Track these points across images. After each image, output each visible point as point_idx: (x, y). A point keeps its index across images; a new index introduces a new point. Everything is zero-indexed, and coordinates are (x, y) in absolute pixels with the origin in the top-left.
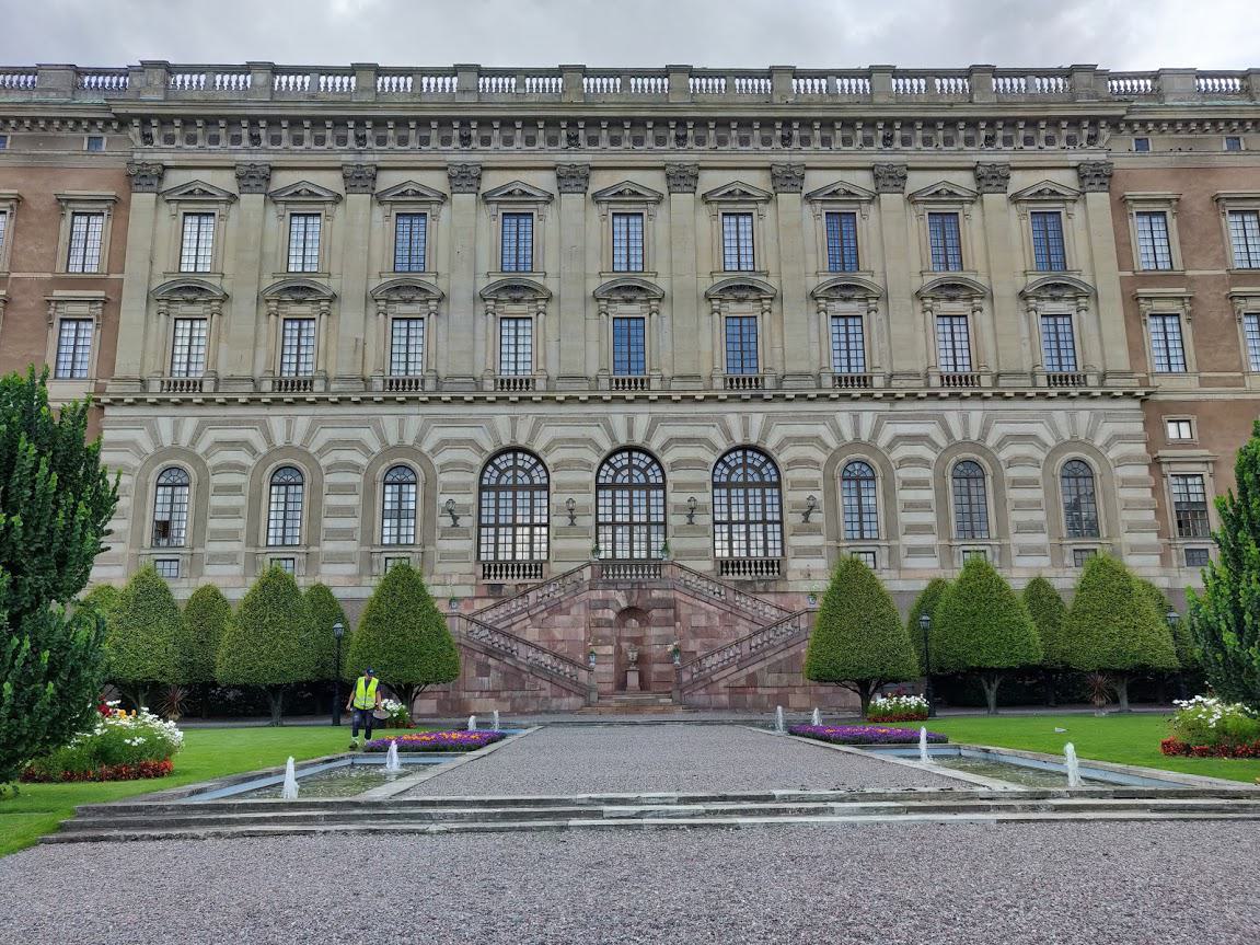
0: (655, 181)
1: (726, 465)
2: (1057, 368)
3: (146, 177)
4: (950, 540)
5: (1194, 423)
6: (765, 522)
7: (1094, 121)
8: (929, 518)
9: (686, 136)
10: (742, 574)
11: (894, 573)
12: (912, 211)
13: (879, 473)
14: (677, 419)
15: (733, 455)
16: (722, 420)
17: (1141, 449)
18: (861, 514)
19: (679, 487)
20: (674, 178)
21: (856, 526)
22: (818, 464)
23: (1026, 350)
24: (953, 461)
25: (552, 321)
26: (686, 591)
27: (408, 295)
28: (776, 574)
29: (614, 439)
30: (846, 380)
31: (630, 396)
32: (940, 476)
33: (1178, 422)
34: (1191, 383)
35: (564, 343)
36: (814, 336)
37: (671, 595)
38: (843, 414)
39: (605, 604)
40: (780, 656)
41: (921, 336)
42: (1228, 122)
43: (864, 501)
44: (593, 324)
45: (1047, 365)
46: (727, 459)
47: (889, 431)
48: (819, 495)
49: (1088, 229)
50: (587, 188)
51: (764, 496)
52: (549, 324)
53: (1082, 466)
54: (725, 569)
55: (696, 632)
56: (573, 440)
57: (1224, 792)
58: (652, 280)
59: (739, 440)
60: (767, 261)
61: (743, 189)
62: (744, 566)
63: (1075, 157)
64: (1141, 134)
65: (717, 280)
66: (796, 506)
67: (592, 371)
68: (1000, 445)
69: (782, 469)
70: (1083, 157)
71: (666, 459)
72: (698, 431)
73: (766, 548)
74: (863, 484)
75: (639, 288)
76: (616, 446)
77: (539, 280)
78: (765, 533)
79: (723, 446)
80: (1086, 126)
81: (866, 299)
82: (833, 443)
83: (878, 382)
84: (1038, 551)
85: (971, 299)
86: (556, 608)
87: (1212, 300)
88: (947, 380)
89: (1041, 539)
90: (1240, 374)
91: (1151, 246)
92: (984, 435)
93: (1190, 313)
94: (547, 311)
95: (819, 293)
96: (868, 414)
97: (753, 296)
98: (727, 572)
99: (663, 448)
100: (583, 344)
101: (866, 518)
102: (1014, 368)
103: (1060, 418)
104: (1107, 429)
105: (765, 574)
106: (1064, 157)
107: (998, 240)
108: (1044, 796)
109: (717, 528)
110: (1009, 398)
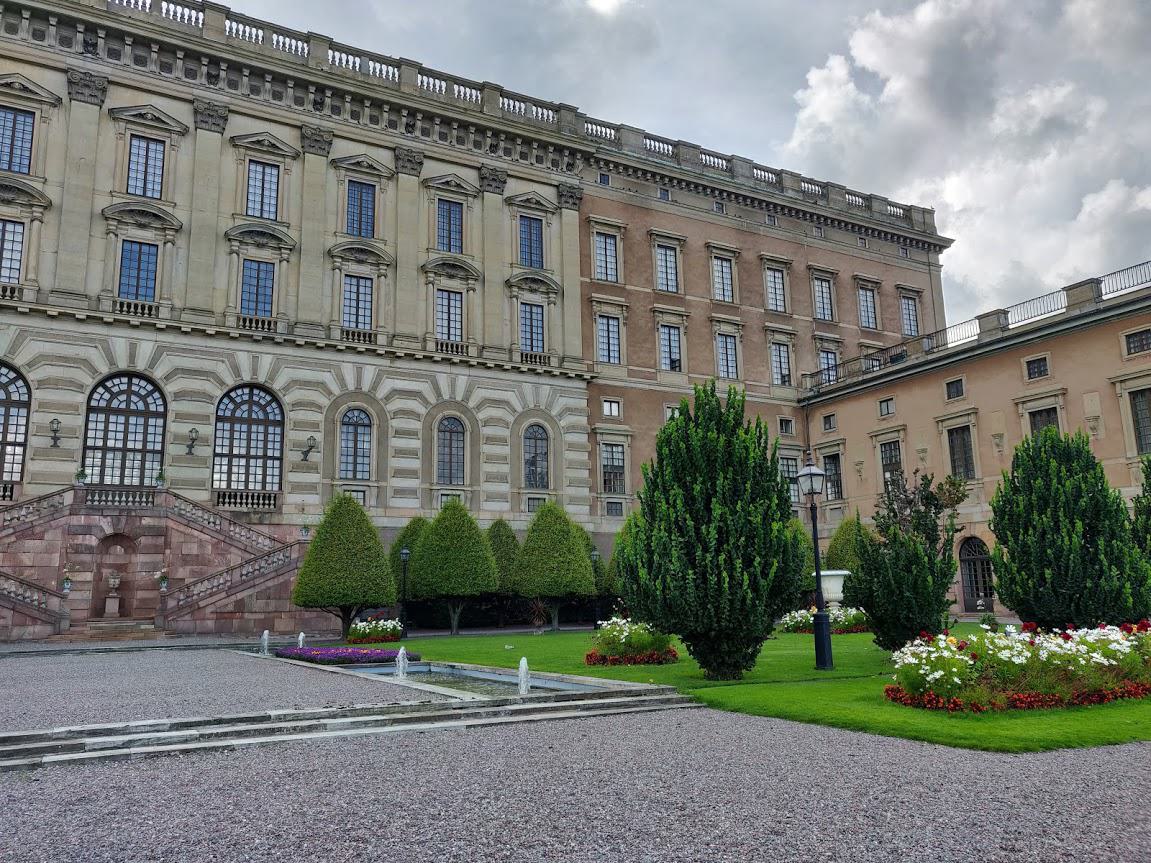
0: (182, 113)
1: (232, 400)
2: (529, 348)
4: (432, 484)
5: (621, 404)
6: (265, 457)
7: (573, 152)
8: (415, 464)
9: (219, 75)
10: (238, 505)
11: (380, 511)
12: (425, 194)
13: (375, 421)
14: (184, 350)
15: (239, 392)
16: (231, 357)
17: (583, 420)
18: (355, 455)
19: (181, 417)
20: (201, 113)
21: (350, 467)
22: (320, 407)
23: (507, 329)
24: (440, 416)
26: (180, 519)
27: (144, 220)
28: (272, 507)
29: (112, 362)
30: (353, 335)
31: (135, 321)
32: (428, 428)
33: (611, 402)
34: (622, 373)
35: (62, 256)
36: (327, 291)
37: (163, 522)
38: (348, 365)
39: (87, 530)
40: (270, 584)
41: (422, 304)
42: (663, 177)
43: (359, 445)
44: (99, 244)
45: (521, 345)
46: (233, 394)
48: (319, 437)
49: (561, 233)
50: (103, 102)
51: (266, 434)
52: (45, 233)
53: (541, 431)
54: (221, 500)
55: (186, 560)
56: (65, 359)
57: (631, 691)
58: (169, 210)
59: (247, 378)
60: (290, 213)
61: (273, 141)
62: (241, 498)
63: (557, 177)
64: (604, 171)
65: (239, 222)
66: (297, 445)
67: (94, 289)
68: (479, 407)
69: (286, 408)
70: (563, 179)
71: (170, 389)
72: (207, 365)
73: (264, 483)
74: (360, 430)
75: (155, 215)
76: (114, 370)
77: (38, 186)
78: (265, 467)
79: (231, 382)
81: (378, 265)
82: (336, 390)
83: (382, 339)
84: (502, 497)
85: (467, 279)
86: (27, 533)
87: (641, 309)
88: (441, 346)
89: (504, 488)
90: (653, 371)
91: (605, 261)
92: (467, 398)
93: (626, 319)
94: (45, 220)
95: (335, 252)
96: (370, 368)
97: (273, 243)
98: (224, 503)
99: (168, 377)
100: (85, 261)
101: (359, 460)
102: (496, 343)
103: (528, 389)
104: (562, 402)
105: (261, 506)
106: (548, 176)
108: (505, 702)
109: (217, 459)
110: (490, 368)
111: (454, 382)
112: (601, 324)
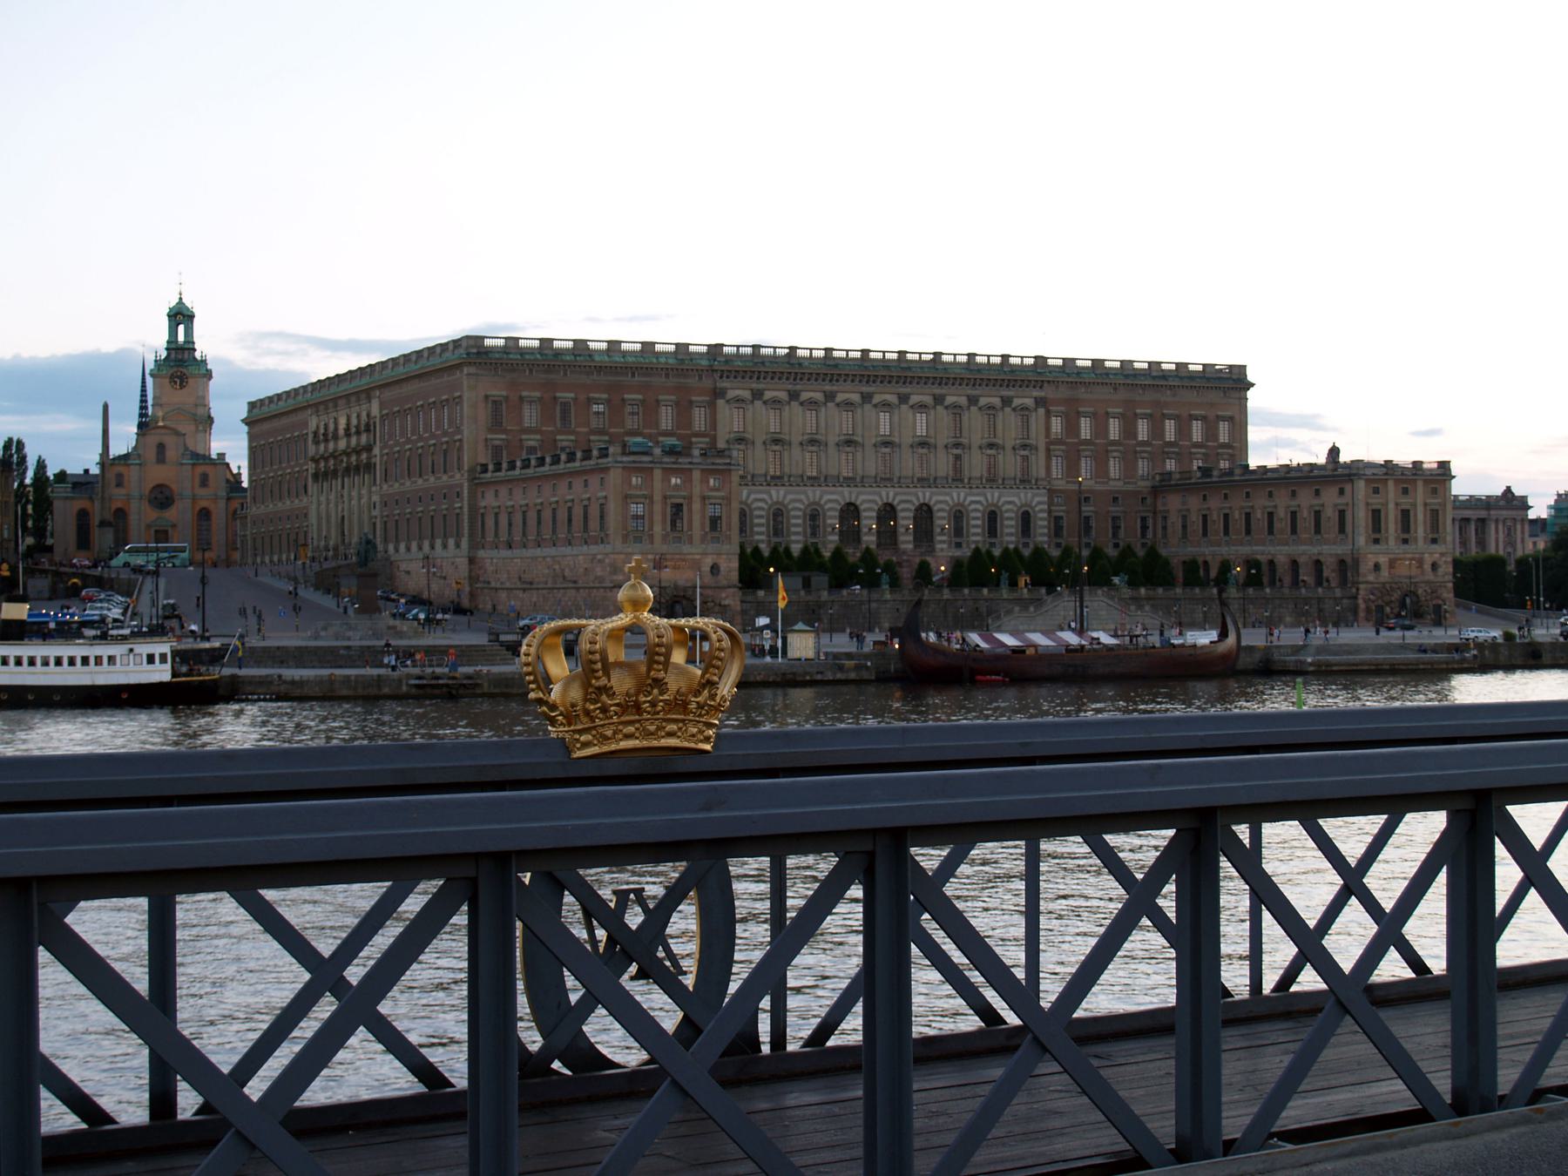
3: (718, 394)
63: (1037, 393)
104: (1037, 499)
111: (993, 495)
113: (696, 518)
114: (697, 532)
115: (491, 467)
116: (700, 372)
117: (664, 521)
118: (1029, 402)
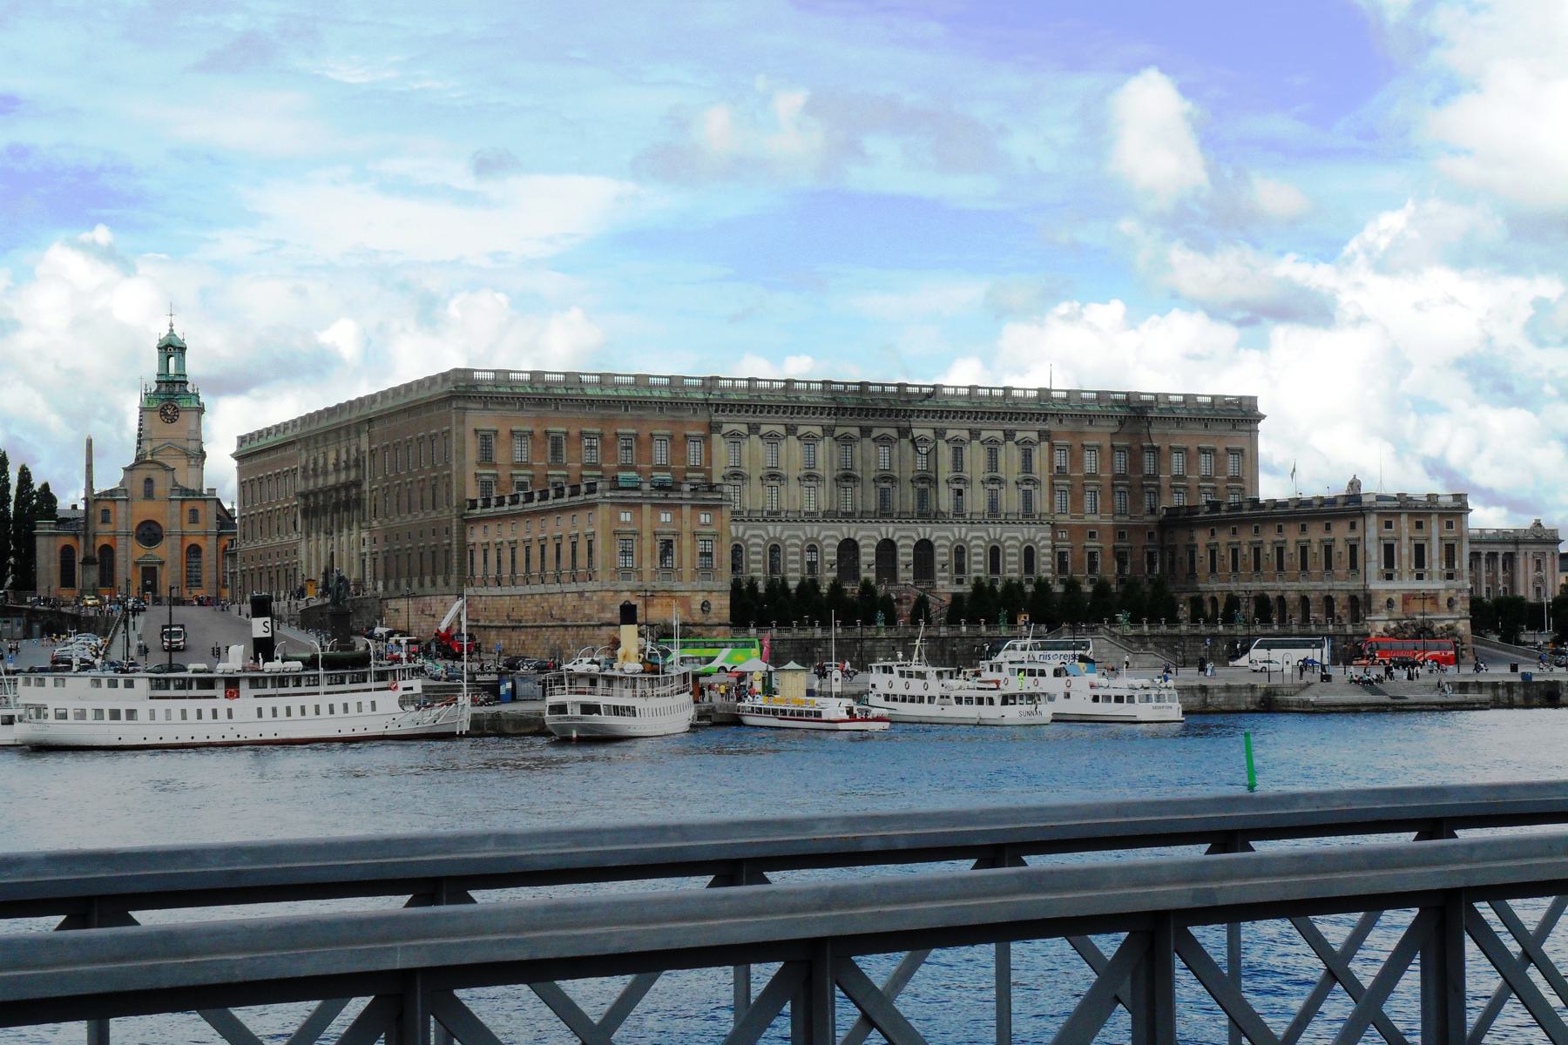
3: (713, 428)
25: (858, 489)
47: (971, 534)
49: (1040, 454)
80: (1043, 416)
91: (1060, 459)
104: (1040, 535)
107: (1010, 459)
111: (995, 531)
112: (1058, 495)
113: (686, 553)
114: (687, 570)
115: (480, 503)
116: (694, 405)
117: (653, 557)
118: (1034, 436)
